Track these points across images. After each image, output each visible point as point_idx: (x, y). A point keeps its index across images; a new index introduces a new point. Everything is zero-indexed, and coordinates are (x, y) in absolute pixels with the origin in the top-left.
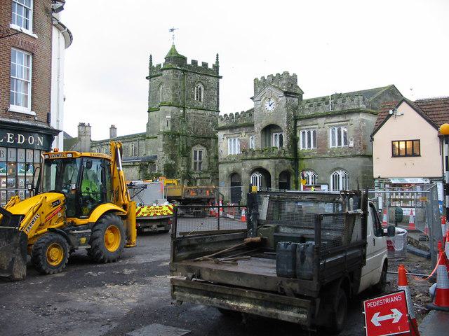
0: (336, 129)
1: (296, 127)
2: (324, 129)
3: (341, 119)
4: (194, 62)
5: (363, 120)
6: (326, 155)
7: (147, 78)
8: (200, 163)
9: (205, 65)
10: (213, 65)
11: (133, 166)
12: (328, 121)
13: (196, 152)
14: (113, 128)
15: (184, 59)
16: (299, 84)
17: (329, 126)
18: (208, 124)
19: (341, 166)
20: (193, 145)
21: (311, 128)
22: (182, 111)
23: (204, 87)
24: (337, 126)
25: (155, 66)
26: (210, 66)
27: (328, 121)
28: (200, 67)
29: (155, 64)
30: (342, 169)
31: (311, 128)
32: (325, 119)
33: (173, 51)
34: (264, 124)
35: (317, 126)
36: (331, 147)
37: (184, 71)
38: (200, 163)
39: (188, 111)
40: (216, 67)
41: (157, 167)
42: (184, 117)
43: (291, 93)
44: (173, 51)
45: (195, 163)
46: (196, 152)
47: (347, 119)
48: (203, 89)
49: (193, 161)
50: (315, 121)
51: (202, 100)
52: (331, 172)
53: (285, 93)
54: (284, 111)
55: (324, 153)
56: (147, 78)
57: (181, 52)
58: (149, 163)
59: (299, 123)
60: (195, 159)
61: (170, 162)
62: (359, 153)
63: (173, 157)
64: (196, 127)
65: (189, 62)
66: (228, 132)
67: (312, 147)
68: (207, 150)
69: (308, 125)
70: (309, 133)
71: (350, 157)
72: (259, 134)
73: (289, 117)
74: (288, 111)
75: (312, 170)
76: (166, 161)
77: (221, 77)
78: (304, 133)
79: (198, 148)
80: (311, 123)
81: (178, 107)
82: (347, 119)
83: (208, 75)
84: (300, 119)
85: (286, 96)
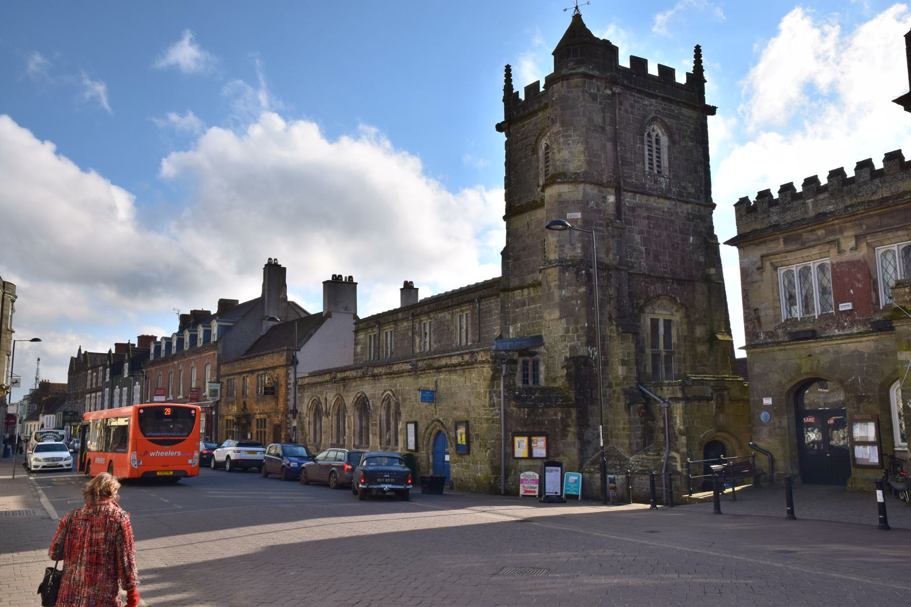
4: (639, 63)
7: (499, 128)
8: (668, 358)
9: (667, 72)
11: (470, 364)
13: (655, 323)
14: (408, 289)
15: (614, 50)
18: (685, 240)
22: (612, 199)
25: (522, 96)
29: (519, 87)
38: (668, 358)
40: (697, 78)
41: (542, 368)
45: (656, 357)
46: (655, 323)
48: (664, 140)
49: (649, 351)
56: (499, 128)
58: (521, 355)
60: (655, 345)
61: (583, 351)
65: (624, 62)
68: (687, 316)
77: (712, 110)
81: (599, 184)
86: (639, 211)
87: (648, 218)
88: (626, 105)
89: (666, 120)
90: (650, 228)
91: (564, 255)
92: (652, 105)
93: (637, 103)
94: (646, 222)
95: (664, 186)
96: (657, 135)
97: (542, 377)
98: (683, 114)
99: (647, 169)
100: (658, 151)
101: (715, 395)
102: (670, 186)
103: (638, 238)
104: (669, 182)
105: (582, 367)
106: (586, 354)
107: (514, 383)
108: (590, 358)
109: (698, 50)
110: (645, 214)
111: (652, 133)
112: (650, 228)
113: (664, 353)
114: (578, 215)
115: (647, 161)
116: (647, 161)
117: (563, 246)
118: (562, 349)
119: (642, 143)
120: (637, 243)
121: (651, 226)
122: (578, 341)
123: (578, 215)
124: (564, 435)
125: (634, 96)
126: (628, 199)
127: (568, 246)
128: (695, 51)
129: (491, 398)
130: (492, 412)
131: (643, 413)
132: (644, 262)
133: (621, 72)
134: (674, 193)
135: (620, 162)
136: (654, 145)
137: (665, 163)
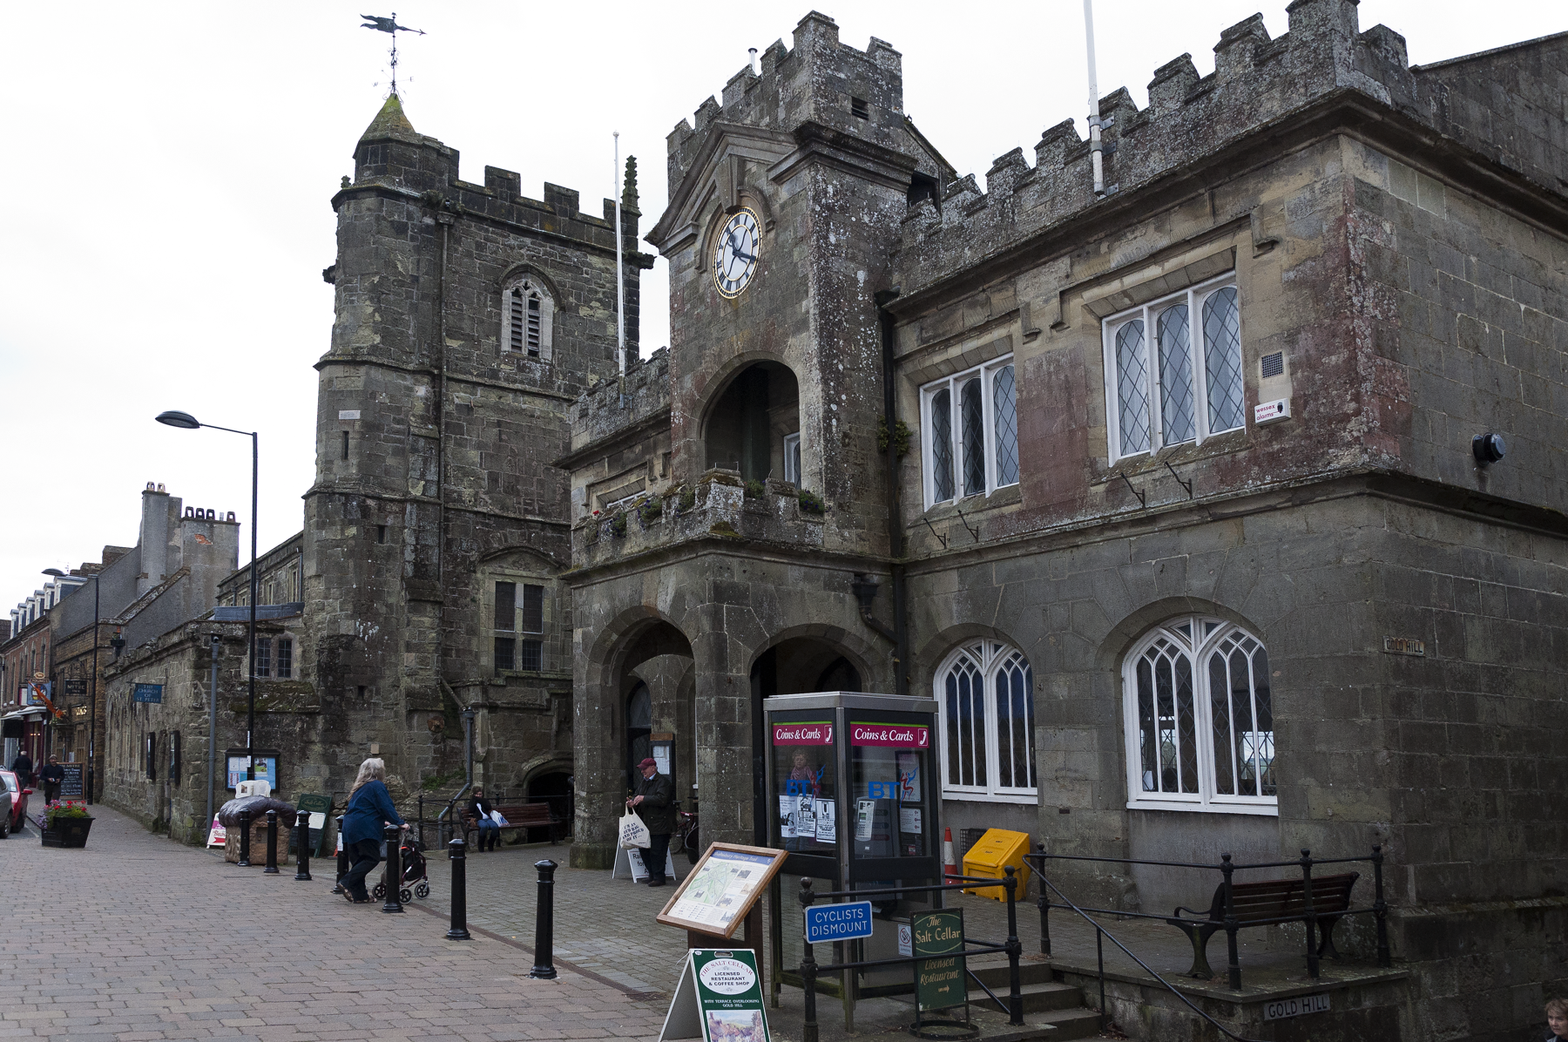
0: (1148, 321)
1: (891, 362)
2: (1063, 342)
3: (1182, 226)
5: (1368, 197)
6: (1083, 518)
9: (561, 199)
10: (609, 206)
12: (1083, 273)
16: (914, 105)
17: (1099, 313)
19: (1198, 584)
20: (487, 557)
21: (979, 356)
23: (562, 308)
24: (1149, 293)
26: (591, 207)
27: (1083, 273)
28: (529, 203)
30: (1208, 610)
31: (979, 356)
32: (1063, 264)
33: (392, 112)
34: (711, 368)
35: (1016, 328)
36: (1114, 456)
37: (430, 205)
39: (459, 396)
41: (297, 651)
42: (437, 421)
43: (841, 141)
44: (392, 112)
47: (1231, 209)
48: (548, 304)
50: (1000, 301)
51: (546, 354)
52: (1121, 641)
53: (806, 136)
54: (804, 259)
55: (1070, 506)
57: (424, 122)
59: (909, 340)
61: (347, 627)
62: (1345, 458)
63: (363, 607)
64: (505, 469)
66: (606, 471)
67: (992, 484)
69: (960, 337)
70: (972, 393)
71: (1266, 503)
72: (696, 438)
73: (831, 291)
74: (823, 252)
75: (999, 637)
76: (334, 621)
78: (942, 402)
79: (520, 576)
80: (976, 317)
82: (1231, 209)
83: (579, 246)
84: (915, 308)
85: (810, 158)
86: (478, 414)
87: (499, 424)
88: (467, 243)
89: (550, 272)
90: (501, 440)
91: (332, 476)
92: (523, 249)
93: (491, 241)
94: (496, 430)
95: (538, 375)
96: (534, 295)
97: (296, 666)
98: (589, 265)
99: (506, 346)
100: (535, 320)
101: (555, 703)
102: (551, 376)
103: (474, 455)
104: (550, 370)
105: (340, 650)
106: (352, 633)
107: (238, 675)
108: (359, 638)
109: (631, 163)
110: (494, 418)
111: (522, 291)
112: (501, 440)
113: (521, 638)
114: (356, 414)
115: (506, 331)
116: (506, 331)
117: (331, 462)
118: (319, 623)
119: (498, 303)
120: (473, 464)
121: (504, 437)
122: (341, 610)
123: (356, 414)
124: (304, 755)
125: (487, 231)
126: (459, 396)
127: (338, 463)
128: (627, 166)
129: (197, 695)
130: (200, 717)
131: (437, 727)
132: (485, 493)
133: (461, 191)
134: (559, 388)
135: (434, 335)
136: (526, 311)
137: (546, 338)
